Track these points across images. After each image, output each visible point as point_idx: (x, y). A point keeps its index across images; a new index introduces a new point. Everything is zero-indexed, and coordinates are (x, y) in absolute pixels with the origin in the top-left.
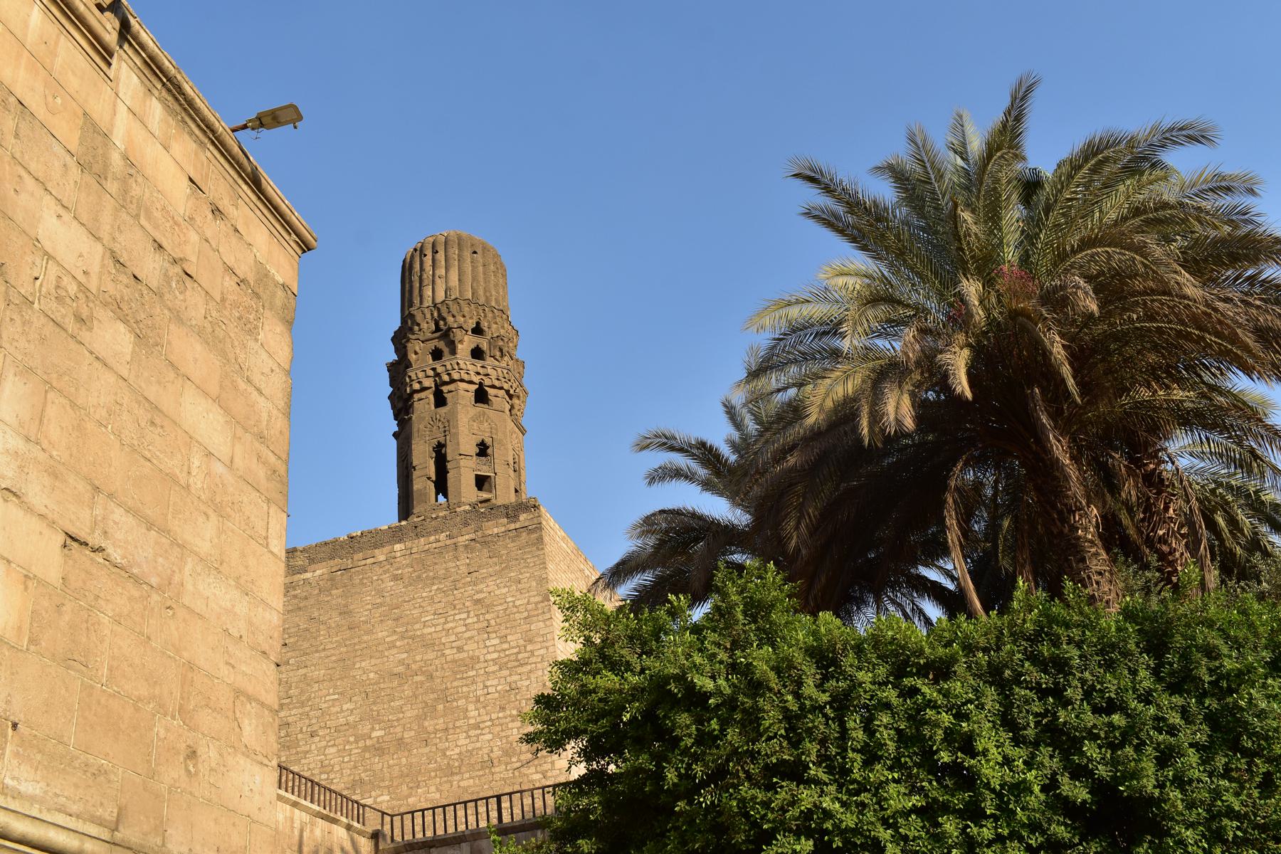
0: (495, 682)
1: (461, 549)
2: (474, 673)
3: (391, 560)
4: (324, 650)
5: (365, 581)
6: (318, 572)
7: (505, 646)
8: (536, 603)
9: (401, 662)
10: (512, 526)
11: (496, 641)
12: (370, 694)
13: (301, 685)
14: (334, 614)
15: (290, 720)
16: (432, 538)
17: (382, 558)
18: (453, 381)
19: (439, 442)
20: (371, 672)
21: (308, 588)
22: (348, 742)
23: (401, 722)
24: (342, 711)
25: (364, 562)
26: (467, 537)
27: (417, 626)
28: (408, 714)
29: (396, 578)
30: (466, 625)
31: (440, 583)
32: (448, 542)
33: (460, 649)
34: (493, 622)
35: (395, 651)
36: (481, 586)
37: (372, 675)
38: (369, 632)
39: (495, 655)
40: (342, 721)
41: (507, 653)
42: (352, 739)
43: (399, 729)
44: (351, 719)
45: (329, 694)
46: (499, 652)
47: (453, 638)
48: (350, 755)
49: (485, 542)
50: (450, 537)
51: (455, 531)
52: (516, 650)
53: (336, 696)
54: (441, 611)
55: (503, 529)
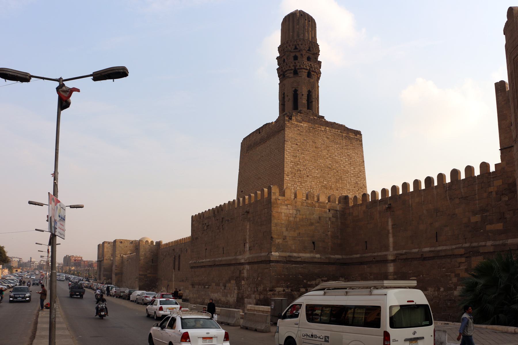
0: (353, 180)
1: (344, 138)
2: (348, 175)
3: (325, 131)
4: (309, 151)
5: (319, 135)
6: (305, 125)
7: (355, 171)
8: (362, 162)
9: (330, 164)
10: (356, 137)
11: (353, 168)
12: (323, 170)
13: (303, 159)
14: (311, 141)
15: (301, 169)
16: (336, 130)
17: (323, 129)
18: (315, 72)
19: (309, 90)
20: (322, 164)
21: (302, 128)
22: (318, 182)
23: (331, 182)
24: (315, 172)
25: (318, 128)
26: (345, 135)
27: (333, 155)
28: (333, 180)
29: (327, 138)
30: (346, 161)
31: (339, 145)
32: (340, 134)
33: (344, 167)
34: (352, 162)
35: (328, 160)
36: (349, 151)
37: (323, 165)
38: (321, 151)
39: (353, 172)
40: (315, 175)
41: (355, 173)
42: (318, 182)
43: (330, 183)
44: (318, 176)
45: (311, 166)
46: (354, 172)
47: (343, 163)
48: (318, 186)
49: (350, 139)
50: (341, 132)
51: (342, 131)
52: (357, 173)
53: (313, 167)
54: (339, 153)
55: (353, 137)
